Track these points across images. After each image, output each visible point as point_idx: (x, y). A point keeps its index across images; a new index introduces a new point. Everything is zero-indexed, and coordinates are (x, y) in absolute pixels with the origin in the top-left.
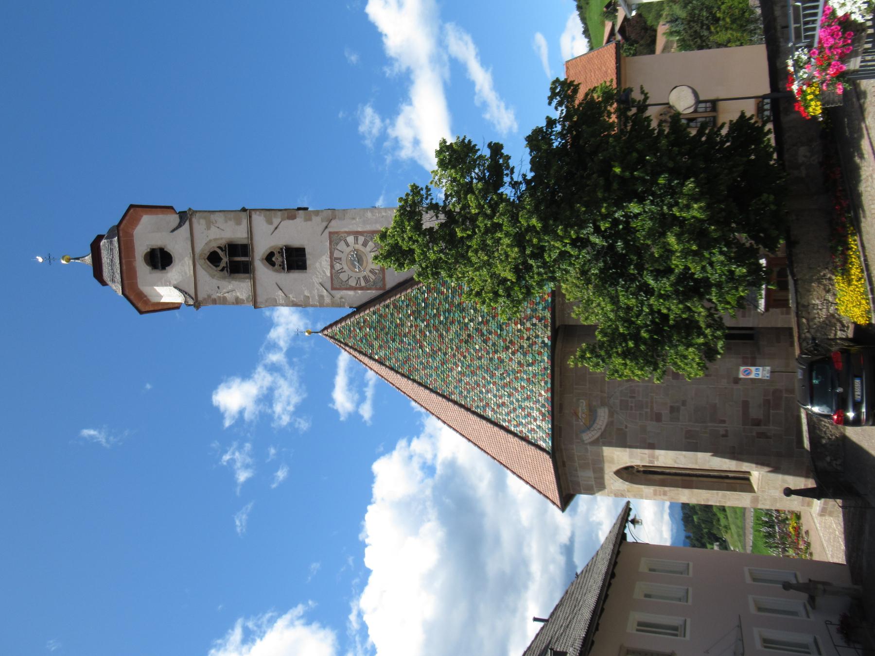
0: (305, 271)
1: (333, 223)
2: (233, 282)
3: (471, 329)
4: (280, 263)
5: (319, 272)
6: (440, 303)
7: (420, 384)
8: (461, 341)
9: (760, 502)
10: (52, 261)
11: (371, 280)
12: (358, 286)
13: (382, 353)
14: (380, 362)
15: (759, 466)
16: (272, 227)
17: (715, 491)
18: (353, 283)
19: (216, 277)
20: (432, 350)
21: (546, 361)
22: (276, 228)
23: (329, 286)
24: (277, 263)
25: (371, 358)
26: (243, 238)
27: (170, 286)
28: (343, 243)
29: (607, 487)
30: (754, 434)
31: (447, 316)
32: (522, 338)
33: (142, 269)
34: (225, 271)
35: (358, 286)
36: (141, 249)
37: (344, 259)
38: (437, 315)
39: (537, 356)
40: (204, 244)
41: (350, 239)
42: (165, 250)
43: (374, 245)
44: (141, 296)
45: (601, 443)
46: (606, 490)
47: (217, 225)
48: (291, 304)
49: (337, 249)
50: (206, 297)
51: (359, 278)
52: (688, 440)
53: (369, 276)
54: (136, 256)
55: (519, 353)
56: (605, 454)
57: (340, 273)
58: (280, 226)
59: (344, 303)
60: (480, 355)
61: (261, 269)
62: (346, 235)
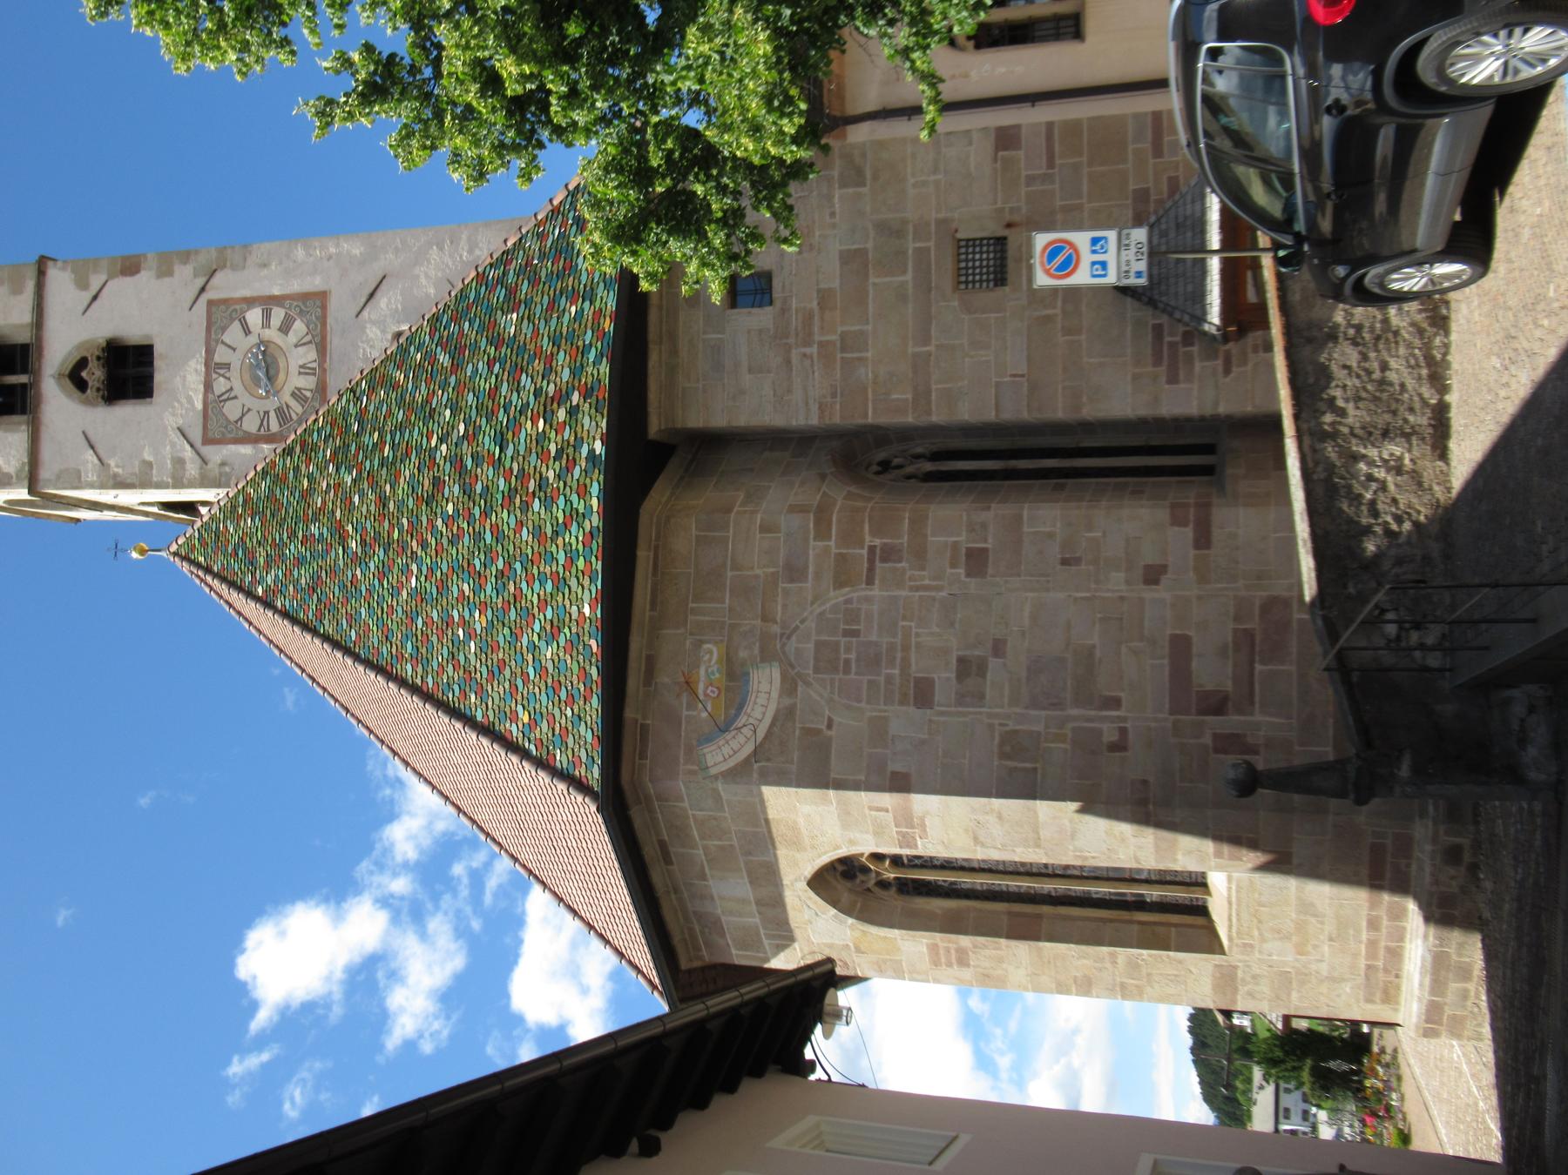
0: (148, 400)
1: (216, 280)
3: (442, 463)
5: (179, 401)
6: (390, 413)
7: (336, 645)
8: (419, 499)
9: (1243, 990)
11: (294, 417)
14: (267, 604)
15: (1226, 849)
16: (88, 296)
17: (1105, 949)
18: (251, 425)
20: (363, 542)
21: (595, 509)
22: (95, 298)
23: (196, 435)
24: (90, 384)
25: (250, 594)
26: (22, 326)
28: (236, 325)
29: (798, 933)
30: (1207, 740)
31: (397, 442)
32: (543, 455)
37: (236, 365)
39: (574, 498)
41: (254, 316)
43: (305, 330)
45: (755, 775)
46: (796, 945)
48: (111, 482)
49: (223, 342)
51: (266, 413)
52: (1003, 762)
53: (288, 406)
55: (537, 500)
56: (772, 814)
57: (225, 401)
59: (228, 476)
61: (57, 402)
62: (245, 306)
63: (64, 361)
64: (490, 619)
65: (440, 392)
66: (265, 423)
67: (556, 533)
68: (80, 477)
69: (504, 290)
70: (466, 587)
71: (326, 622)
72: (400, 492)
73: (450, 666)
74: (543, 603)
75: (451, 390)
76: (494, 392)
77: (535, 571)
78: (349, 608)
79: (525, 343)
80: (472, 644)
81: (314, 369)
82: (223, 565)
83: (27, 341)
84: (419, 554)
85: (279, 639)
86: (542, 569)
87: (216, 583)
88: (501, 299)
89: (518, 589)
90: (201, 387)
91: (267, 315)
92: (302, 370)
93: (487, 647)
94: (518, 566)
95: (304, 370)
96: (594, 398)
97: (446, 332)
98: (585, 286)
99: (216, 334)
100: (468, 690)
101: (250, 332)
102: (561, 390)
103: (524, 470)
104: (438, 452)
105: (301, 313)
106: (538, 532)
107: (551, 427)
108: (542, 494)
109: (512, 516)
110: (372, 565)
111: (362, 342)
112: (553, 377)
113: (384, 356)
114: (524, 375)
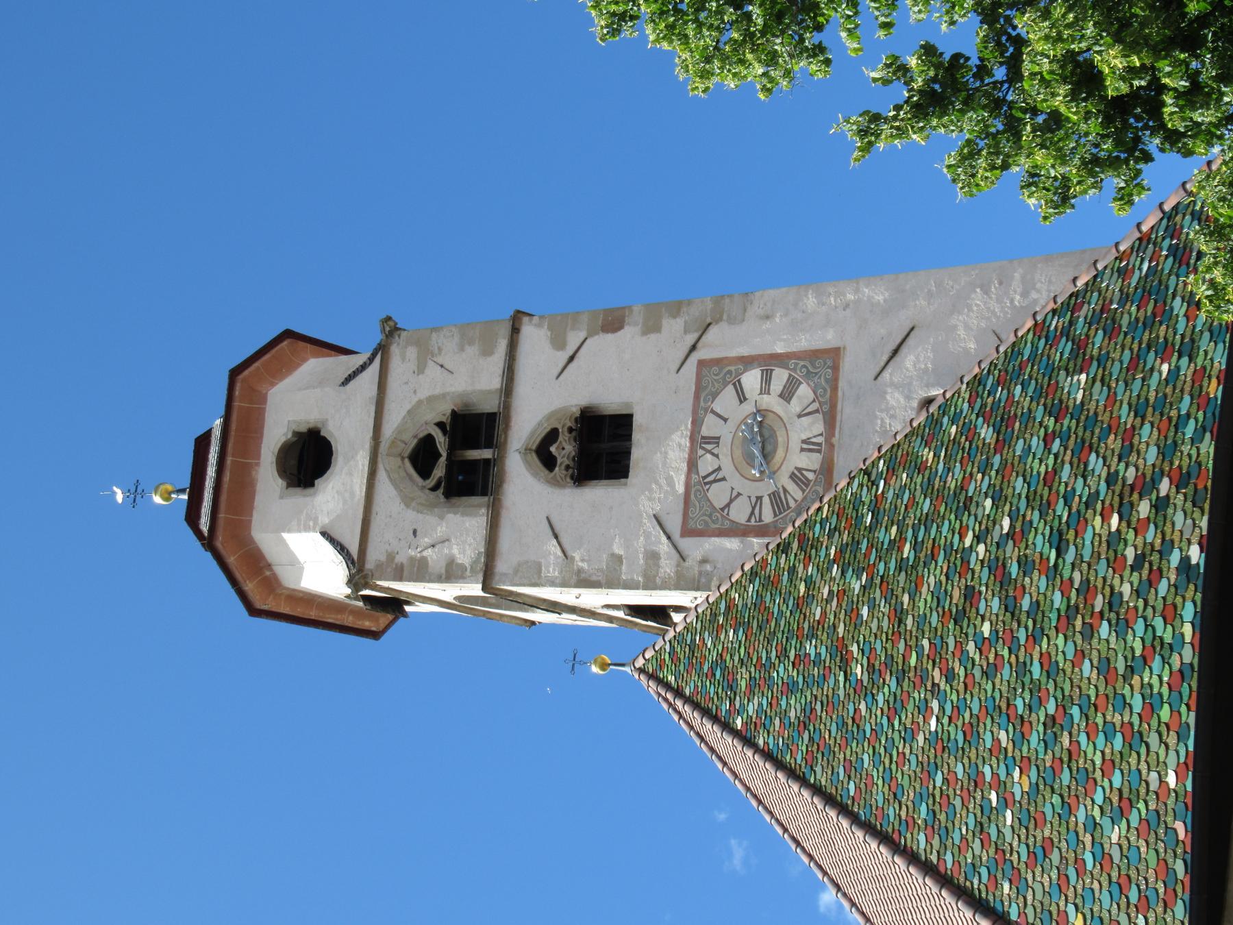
1: (713, 334)
2: (451, 518)
3: (978, 568)
4: (567, 462)
6: (913, 501)
7: (830, 800)
10: (139, 497)
11: (792, 504)
12: (753, 522)
14: (748, 741)
16: (563, 356)
18: (739, 513)
19: (413, 504)
20: (871, 668)
21: (1188, 639)
22: (572, 359)
23: (675, 525)
25: (727, 727)
26: (490, 392)
27: (314, 530)
28: (731, 387)
31: (920, 539)
32: (1116, 562)
35: (753, 522)
37: (726, 439)
38: (897, 544)
39: (1158, 622)
40: (403, 413)
42: (322, 433)
43: (812, 396)
44: (257, 563)
47: (440, 360)
49: (713, 412)
50: (383, 558)
51: (759, 498)
53: (785, 491)
54: (263, 451)
55: (1105, 623)
57: (711, 483)
59: (709, 576)
60: (992, 657)
63: (533, 433)
64: (1034, 781)
65: (980, 475)
66: (757, 511)
67: (1131, 670)
68: (540, 571)
69: (1070, 344)
70: (1003, 736)
71: (818, 769)
72: (922, 604)
73: (977, 841)
74: (1109, 765)
75: (993, 473)
76: (1050, 478)
77: (1099, 720)
78: (848, 753)
79: (1096, 414)
80: (1009, 814)
81: (819, 444)
82: (696, 687)
83: (495, 410)
84: (942, 687)
85: (758, 786)
86: (1109, 718)
87: (687, 710)
88: (1066, 355)
89: (1075, 742)
90: (684, 466)
91: (767, 378)
92: (805, 446)
93: (1030, 819)
94: (1075, 711)
95: (808, 446)
96: (1191, 487)
97: (990, 399)
98: (1183, 336)
99: (706, 401)
100: (999, 876)
101: (745, 399)
102: (1144, 475)
103: (1088, 581)
104: (974, 554)
105: (809, 375)
106: (1105, 668)
107: (1129, 526)
108: (1113, 615)
109: (1070, 644)
110: (880, 698)
111: (881, 411)
112: (1133, 458)
113: (908, 429)
114: (1093, 456)
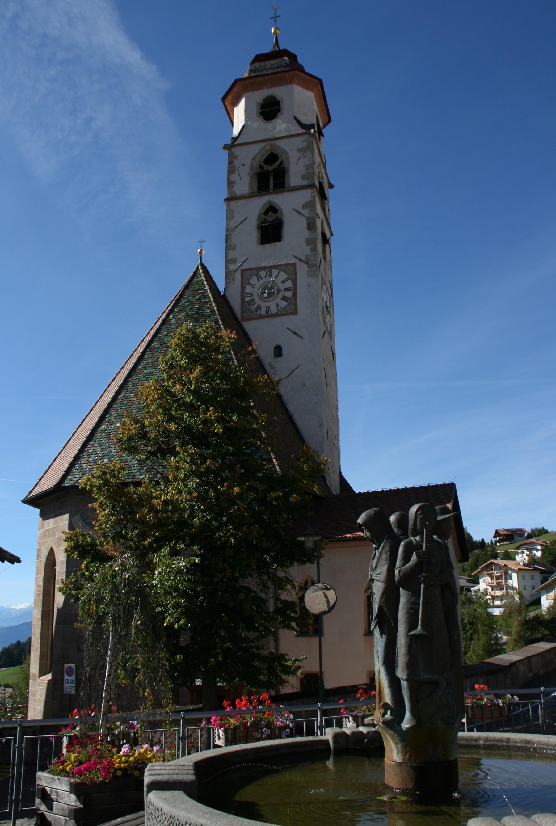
0: (260, 243)
1: (305, 267)
11: (251, 307)
13: (173, 321)
16: (300, 209)
17: (39, 641)
18: (248, 289)
22: (299, 213)
23: (245, 267)
24: (267, 216)
28: (287, 277)
33: (261, 95)
34: (259, 170)
36: (278, 92)
40: (284, 147)
42: (279, 114)
43: (283, 307)
47: (301, 158)
50: (235, 154)
51: (252, 295)
53: (255, 304)
58: (302, 216)
61: (260, 203)
63: (275, 203)
68: (231, 219)
81: (268, 313)
95: (268, 309)
101: (283, 283)
